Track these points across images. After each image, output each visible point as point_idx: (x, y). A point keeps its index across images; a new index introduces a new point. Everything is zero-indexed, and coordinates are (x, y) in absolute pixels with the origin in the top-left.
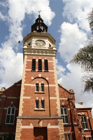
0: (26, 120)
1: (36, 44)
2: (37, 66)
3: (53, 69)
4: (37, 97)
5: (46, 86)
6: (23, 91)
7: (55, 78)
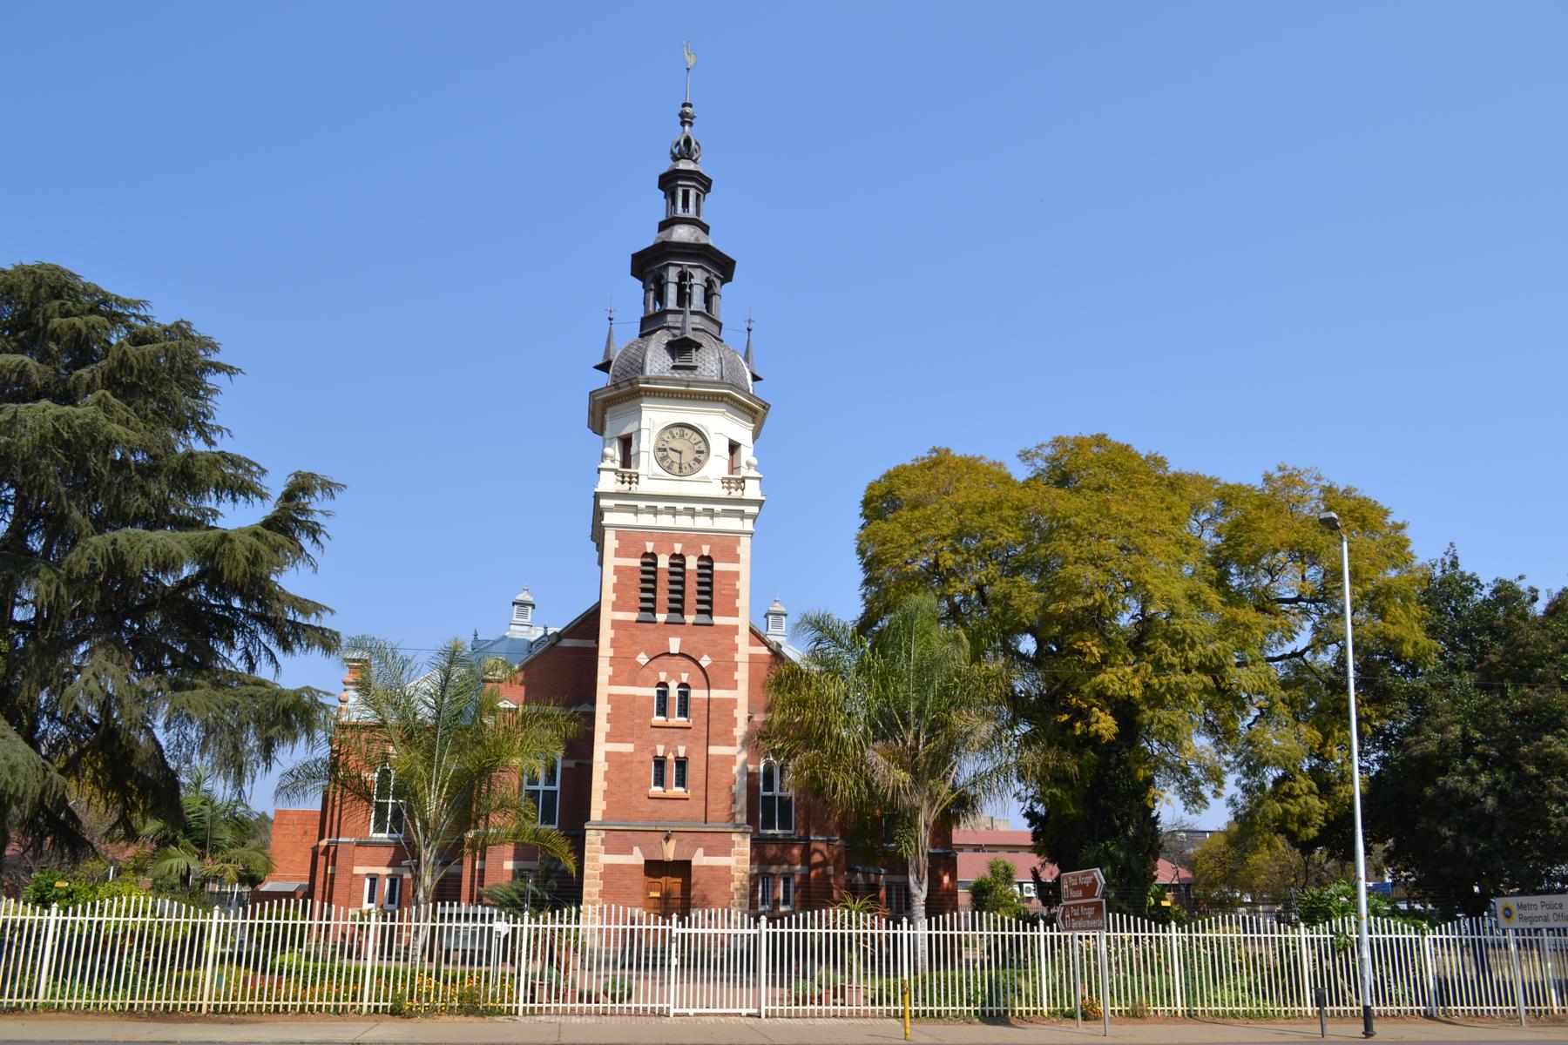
0: (618, 839)
1: (662, 453)
2: (663, 596)
3: (734, 612)
4: (659, 742)
5: (697, 694)
6: (604, 718)
7: (737, 657)
